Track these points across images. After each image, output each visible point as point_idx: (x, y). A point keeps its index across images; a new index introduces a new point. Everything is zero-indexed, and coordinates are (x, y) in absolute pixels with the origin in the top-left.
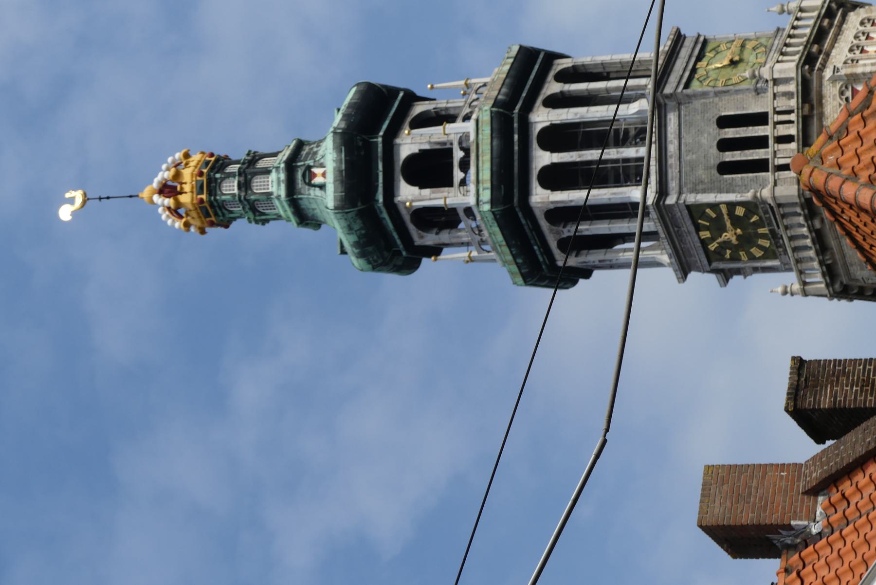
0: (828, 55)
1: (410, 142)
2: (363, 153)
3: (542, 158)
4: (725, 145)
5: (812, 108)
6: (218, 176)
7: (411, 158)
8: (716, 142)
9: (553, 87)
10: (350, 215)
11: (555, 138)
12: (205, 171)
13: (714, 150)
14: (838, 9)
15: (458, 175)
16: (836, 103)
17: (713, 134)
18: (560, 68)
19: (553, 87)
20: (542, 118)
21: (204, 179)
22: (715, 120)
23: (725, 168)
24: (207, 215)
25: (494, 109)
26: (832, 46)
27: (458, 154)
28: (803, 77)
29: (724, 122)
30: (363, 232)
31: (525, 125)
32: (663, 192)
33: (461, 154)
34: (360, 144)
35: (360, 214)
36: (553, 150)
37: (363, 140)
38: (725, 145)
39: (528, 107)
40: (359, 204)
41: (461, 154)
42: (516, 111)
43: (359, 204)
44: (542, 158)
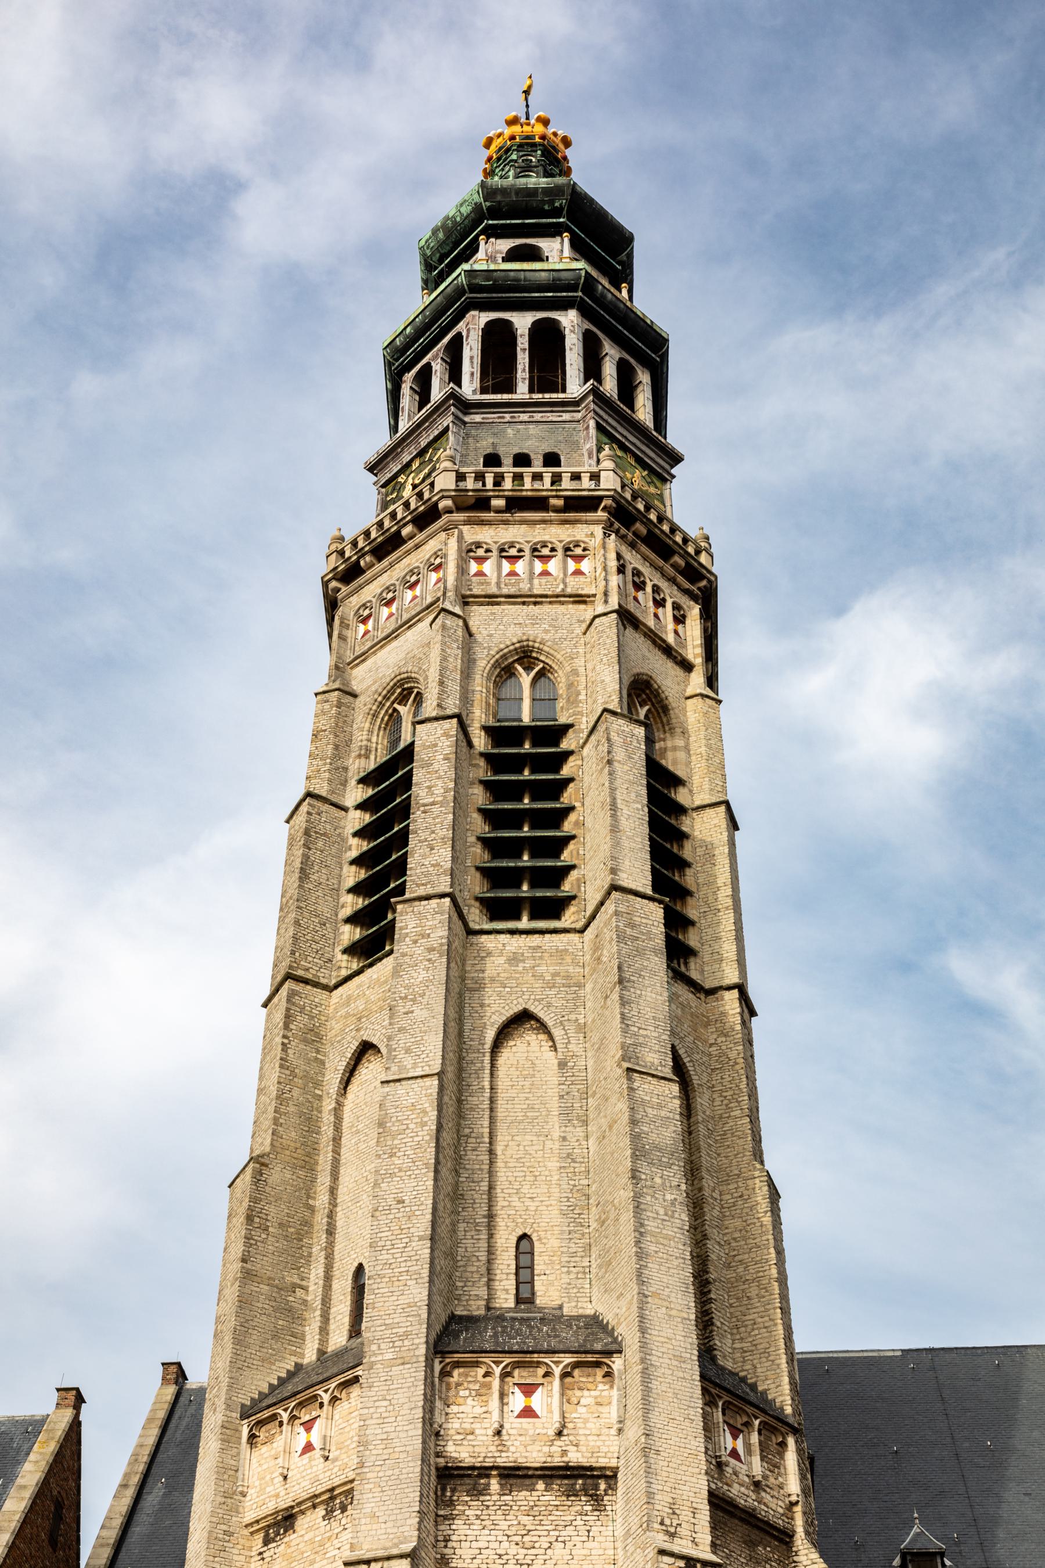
0: (632, 545)
2: (546, 207)
3: (522, 322)
5: (557, 510)
6: (539, 152)
8: (525, 451)
9: (611, 355)
10: (476, 196)
11: (547, 338)
13: (516, 450)
14: (699, 589)
16: (563, 537)
17: (536, 446)
18: (639, 372)
22: (556, 450)
25: (583, 273)
26: (645, 558)
28: (600, 499)
30: (458, 219)
31: (563, 305)
32: (466, 406)
34: (557, 204)
35: (478, 207)
37: (561, 208)
39: (585, 312)
40: (488, 204)
43: (488, 204)
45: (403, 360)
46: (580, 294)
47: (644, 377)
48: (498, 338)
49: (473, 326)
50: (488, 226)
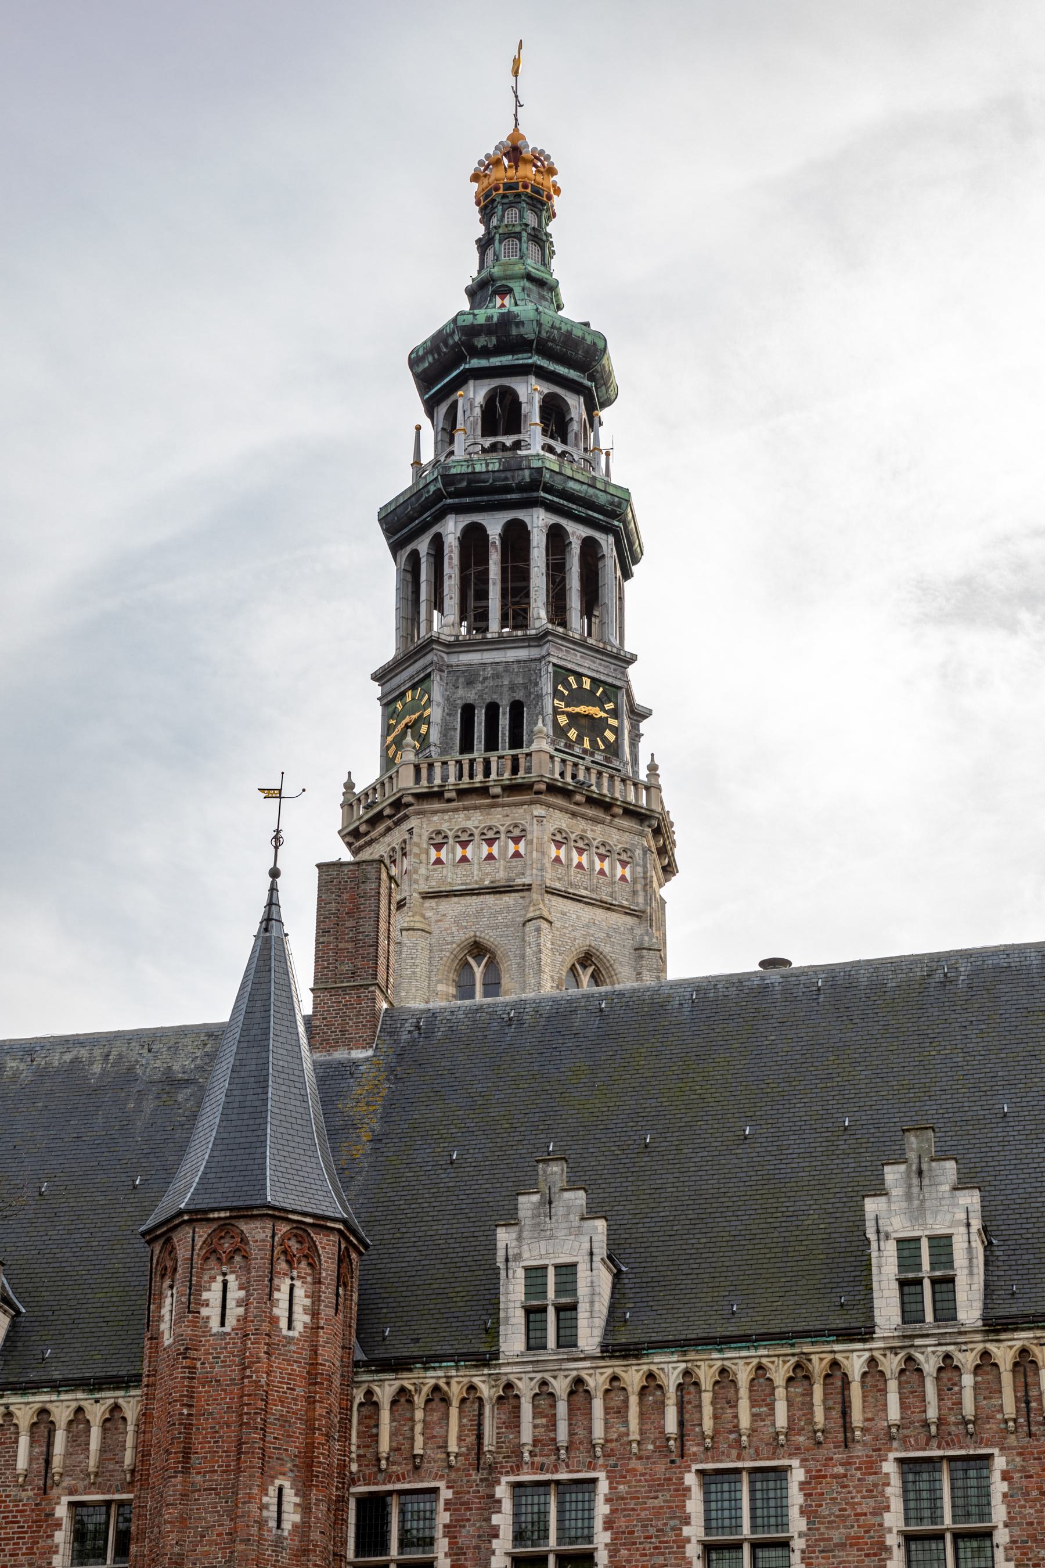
1: (530, 392)
3: (494, 526)
4: (492, 710)
7: (515, 396)
9: (576, 532)
11: (516, 538)
12: (529, 191)
15: (488, 442)
19: (576, 532)
20: (538, 521)
21: (521, 189)
23: (468, 711)
24: (487, 196)
27: (508, 440)
29: (517, 708)
33: (508, 443)
36: (504, 537)
38: (492, 710)
41: (508, 443)
42: (542, 494)
44: (494, 526)
45: (405, 524)
46: (542, 494)
47: (607, 543)
48: (474, 541)
49: (452, 529)
50: (465, 371)
